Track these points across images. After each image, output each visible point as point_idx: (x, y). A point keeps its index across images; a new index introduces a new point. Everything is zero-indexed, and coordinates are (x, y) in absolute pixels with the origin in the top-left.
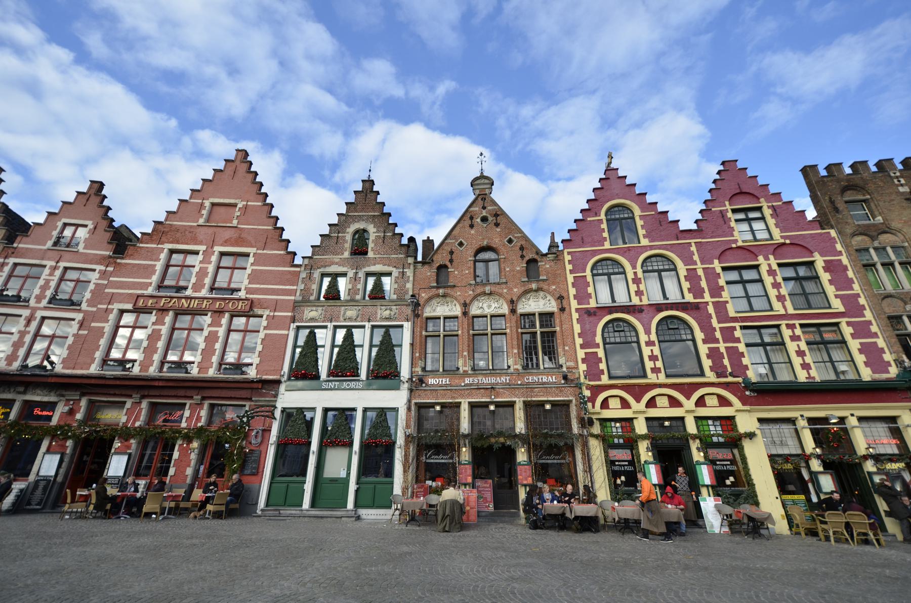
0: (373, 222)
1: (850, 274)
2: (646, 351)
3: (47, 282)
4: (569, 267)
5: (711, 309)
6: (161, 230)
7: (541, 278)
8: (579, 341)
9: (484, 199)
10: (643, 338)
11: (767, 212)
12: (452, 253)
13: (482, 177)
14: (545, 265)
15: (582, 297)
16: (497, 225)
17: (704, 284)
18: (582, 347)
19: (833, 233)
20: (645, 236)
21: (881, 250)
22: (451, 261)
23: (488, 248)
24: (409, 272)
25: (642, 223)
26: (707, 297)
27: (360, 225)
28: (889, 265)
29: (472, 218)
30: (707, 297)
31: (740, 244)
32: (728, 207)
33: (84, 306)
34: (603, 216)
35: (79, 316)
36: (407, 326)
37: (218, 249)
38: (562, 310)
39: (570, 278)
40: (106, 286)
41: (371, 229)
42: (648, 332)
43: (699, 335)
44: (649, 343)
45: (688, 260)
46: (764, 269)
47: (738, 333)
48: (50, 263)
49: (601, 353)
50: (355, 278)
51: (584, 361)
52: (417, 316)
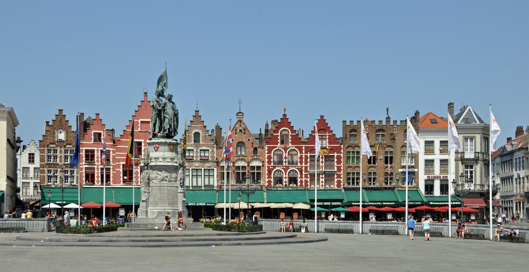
0: (201, 129)
1: (342, 160)
2: (284, 180)
3: (98, 155)
4: (267, 152)
5: (303, 168)
7: (258, 154)
8: (267, 176)
9: (240, 122)
10: (284, 176)
11: (328, 137)
15: (269, 162)
16: (245, 133)
17: (304, 160)
18: (268, 178)
19: (342, 147)
20: (291, 143)
21: (353, 152)
23: (242, 142)
24: (215, 150)
25: (290, 137)
26: (303, 165)
27: (197, 131)
28: (353, 157)
29: (236, 130)
30: (303, 165)
33: (111, 163)
34: (279, 134)
36: (215, 169)
38: (263, 166)
39: (267, 156)
40: (115, 156)
41: (200, 132)
42: (286, 174)
43: (299, 176)
44: (286, 178)
45: (301, 152)
48: (96, 149)
49: (272, 180)
50: (197, 152)
51: (267, 182)
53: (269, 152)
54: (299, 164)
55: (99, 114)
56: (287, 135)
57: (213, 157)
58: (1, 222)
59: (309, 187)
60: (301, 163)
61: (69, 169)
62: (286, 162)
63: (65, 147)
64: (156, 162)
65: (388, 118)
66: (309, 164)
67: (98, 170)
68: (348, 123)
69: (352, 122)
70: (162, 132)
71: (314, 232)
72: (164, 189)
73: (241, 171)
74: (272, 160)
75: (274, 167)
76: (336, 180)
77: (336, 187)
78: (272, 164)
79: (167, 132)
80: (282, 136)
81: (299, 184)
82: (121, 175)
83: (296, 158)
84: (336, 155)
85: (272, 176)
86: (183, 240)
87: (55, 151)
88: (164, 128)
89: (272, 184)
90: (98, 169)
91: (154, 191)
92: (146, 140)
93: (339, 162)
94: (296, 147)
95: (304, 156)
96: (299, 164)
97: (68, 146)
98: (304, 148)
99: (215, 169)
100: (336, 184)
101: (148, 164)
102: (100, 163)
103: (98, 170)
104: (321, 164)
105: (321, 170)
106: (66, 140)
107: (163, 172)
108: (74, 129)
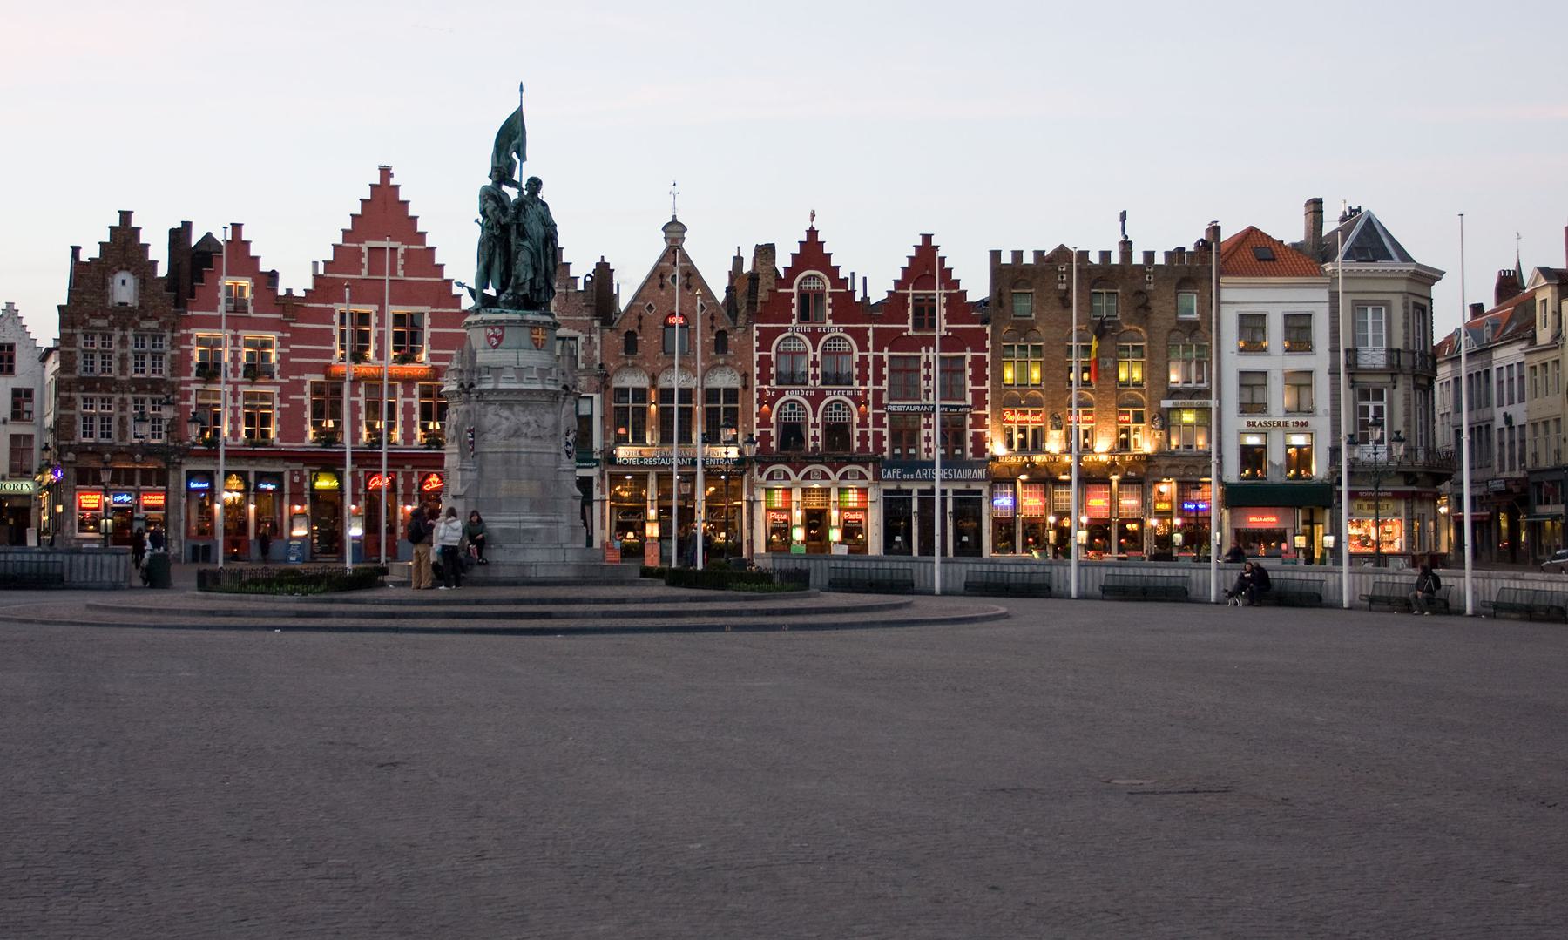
1: (988, 371)
2: (811, 432)
6: (324, 286)
7: (731, 352)
8: (756, 420)
10: (811, 420)
12: (640, 318)
13: (674, 221)
14: (733, 339)
15: (764, 378)
17: (870, 371)
18: (758, 426)
19: (988, 330)
22: (640, 327)
24: (596, 338)
29: (662, 276)
31: (911, 333)
32: (911, 291)
33: (277, 378)
34: (795, 290)
35: (275, 390)
36: (597, 397)
37: (393, 310)
38: (745, 387)
42: (815, 415)
43: (856, 419)
44: (815, 425)
45: (863, 347)
46: (923, 359)
47: (886, 420)
52: (607, 387)
53: (765, 343)
54: (856, 383)
55: (240, 225)
56: (820, 295)
57: (589, 359)
58: (2, 557)
59: (886, 454)
60: (863, 379)
61: (148, 396)
62: (815, 377)
63: (136, 325)
64: (497, 381)
65: (1126, 246)
66: (885, 383)
67: (235, 400)
68: (1006, 259)
69: (1018, 255)
70: (510, 290)
71: (932, 593)
72: (518, 460)
73: (676, 405)
74: (773, 370)
75: (780, 393)
76: (970, 433)
77: (970, 455)
78: (773, 382)
79: (526, 289)
80: (804, 297)
81: (856, 444)
82: (308, 414)
83: (851, 365)
84: (969, 355)
85: (773, 419)
86: (605, 615)
87: (107, 337)
88: (518, 278)
89: (773, 444)
90: (235, 394)
91: (488, 469)
92: (382, 306)
93: (979, 378)
94: (846, 330)
95: (870, 359)
96: (856, 383)
97: (146, 324)
98: (870, 333)
99: (597, 397)
100: (969, 445)
101: (472, 385)
102: (241, 377)
103: (235, 400)
104: (923, 383)
105: (924, 401)
106: (141, 307)
107: (517, 409)
108: (162, 271)
